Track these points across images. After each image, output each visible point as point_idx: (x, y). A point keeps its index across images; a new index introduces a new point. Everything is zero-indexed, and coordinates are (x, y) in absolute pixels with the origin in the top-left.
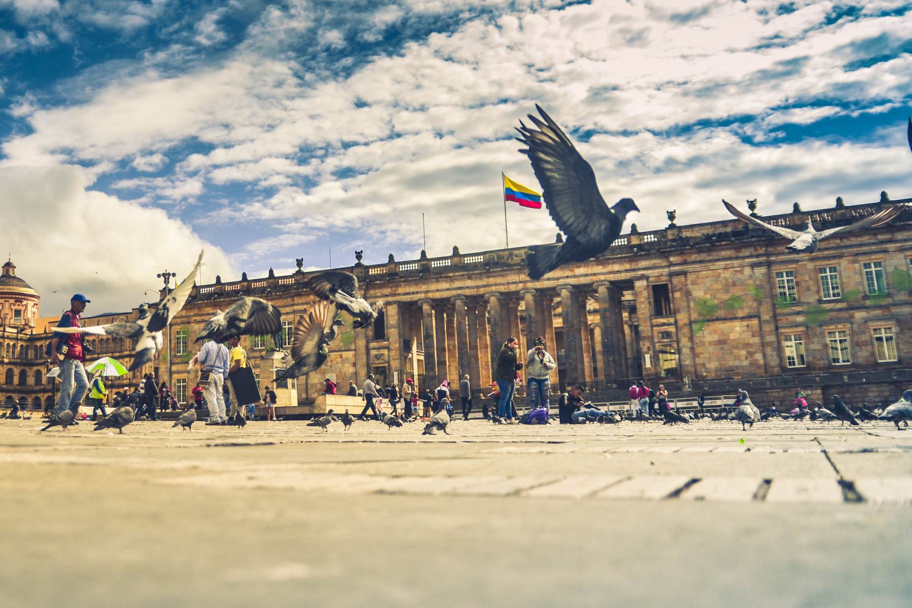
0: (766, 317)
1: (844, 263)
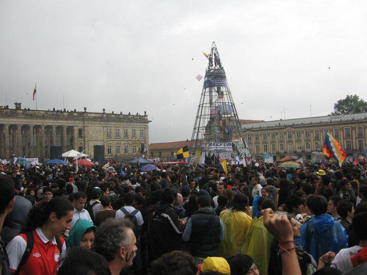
0: (105, 141)
1: (121, 128)
